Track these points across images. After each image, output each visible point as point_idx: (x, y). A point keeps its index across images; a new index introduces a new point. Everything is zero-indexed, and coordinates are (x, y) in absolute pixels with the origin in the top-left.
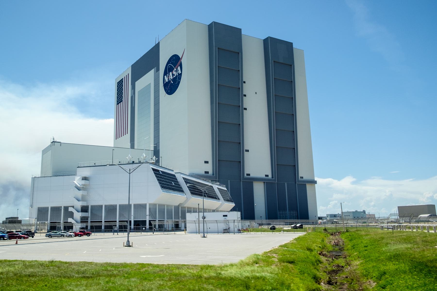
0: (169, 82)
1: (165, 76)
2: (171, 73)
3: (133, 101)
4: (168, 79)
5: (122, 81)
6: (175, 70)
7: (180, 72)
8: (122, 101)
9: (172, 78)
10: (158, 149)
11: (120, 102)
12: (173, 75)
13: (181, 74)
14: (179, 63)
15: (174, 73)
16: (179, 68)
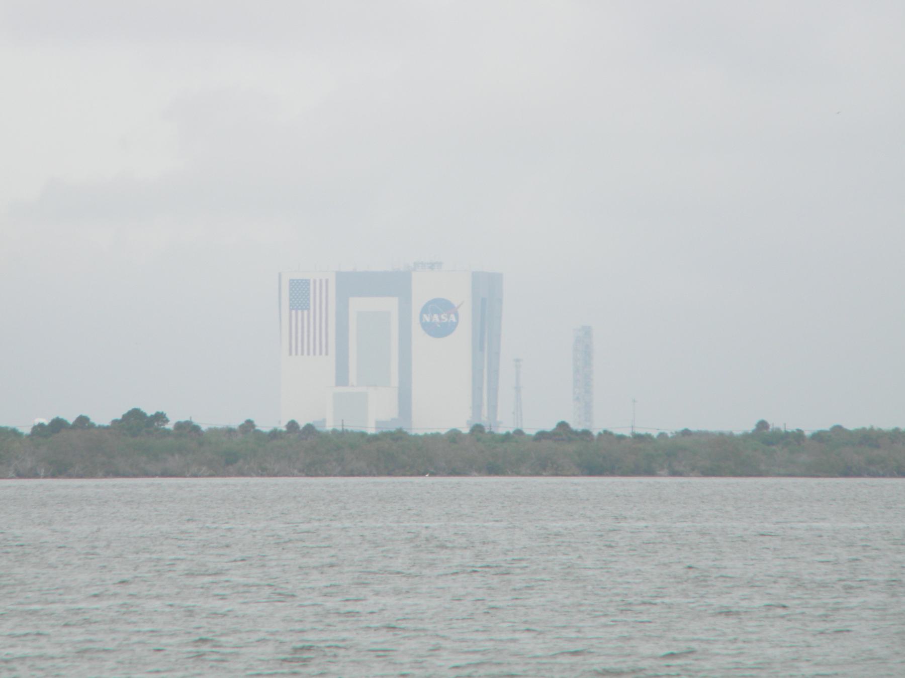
2: (436, 316)
4: (431, 320)
5: (309, 284)
7: (454, 320)
8: (308, 309)
12: (440, 319)
13: (456, 324)
15: (442, 317)
16: (452, 316)
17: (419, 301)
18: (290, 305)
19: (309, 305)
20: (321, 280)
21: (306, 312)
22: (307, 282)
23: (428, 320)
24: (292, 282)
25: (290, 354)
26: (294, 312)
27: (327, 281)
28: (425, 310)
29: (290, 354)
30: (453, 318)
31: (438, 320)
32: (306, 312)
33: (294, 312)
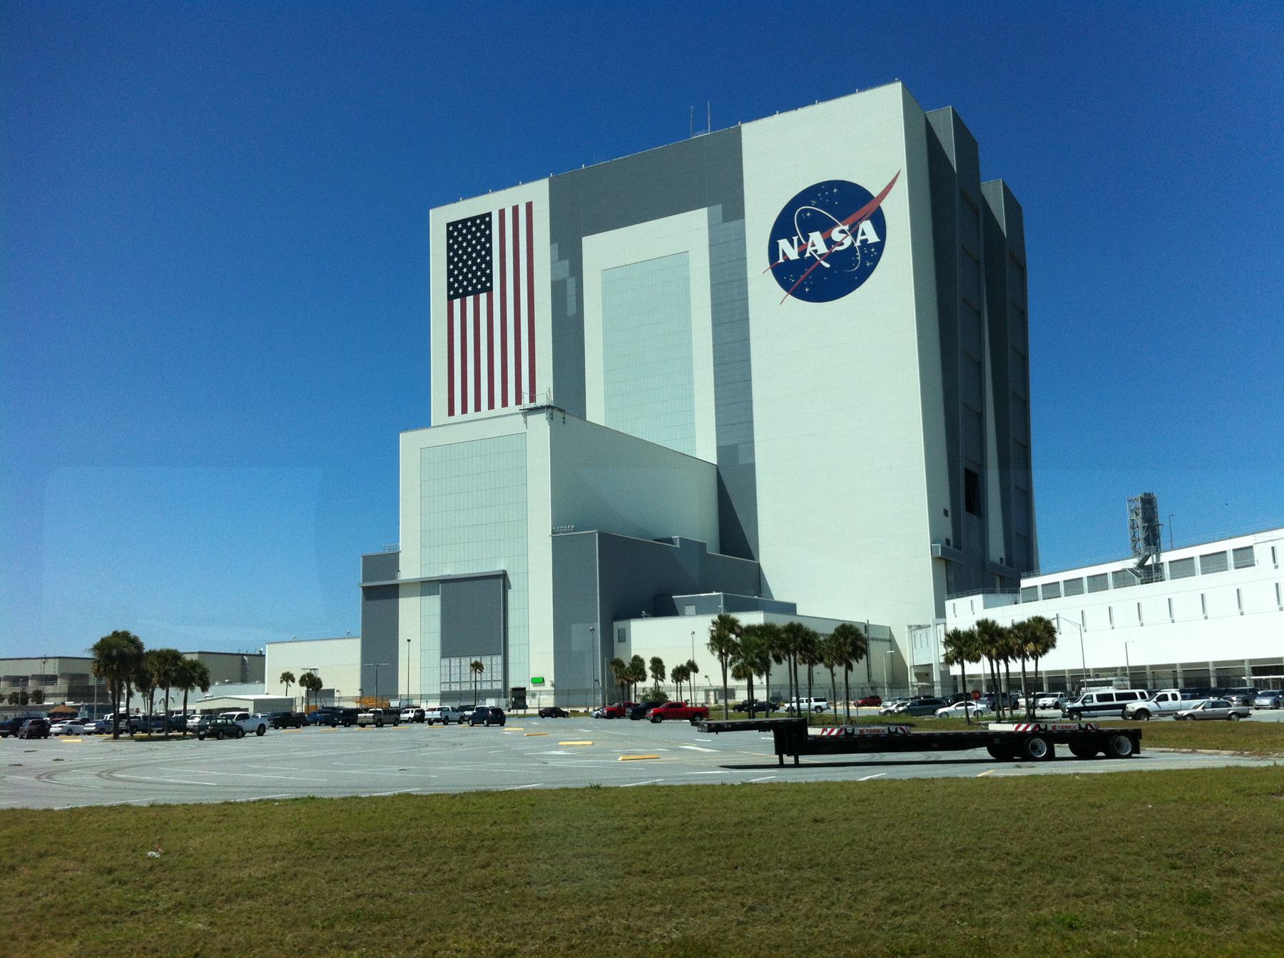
0: (805, 262)
1: (783, 244)
2: (816, 237)
3: (571, 300)
4: (802, 253)
5: (489, 225)
6: (846, 228)
7: (872, 237)
9: (825, 250)
10: (741, 461)
11: (476, 293)
12: (829, 242)
13: (880, 247)
14: (868, 208)
15: (836, 235)
16: (867, 226)
17: (764, 200)
18: (450, 286)
19: (490, 278)
20: (515, 210)
21: (483, 297)
22: (485, 219)
23: (793, 254)
24: (454, 229)
25: (451, 413)
26: (457, 302)
27: (529, 206)
28: (783, 228)
29: (451, 413)
30: (868, 231)
31: (822, 248)
32: (483, 297)
33: (457, 302)
